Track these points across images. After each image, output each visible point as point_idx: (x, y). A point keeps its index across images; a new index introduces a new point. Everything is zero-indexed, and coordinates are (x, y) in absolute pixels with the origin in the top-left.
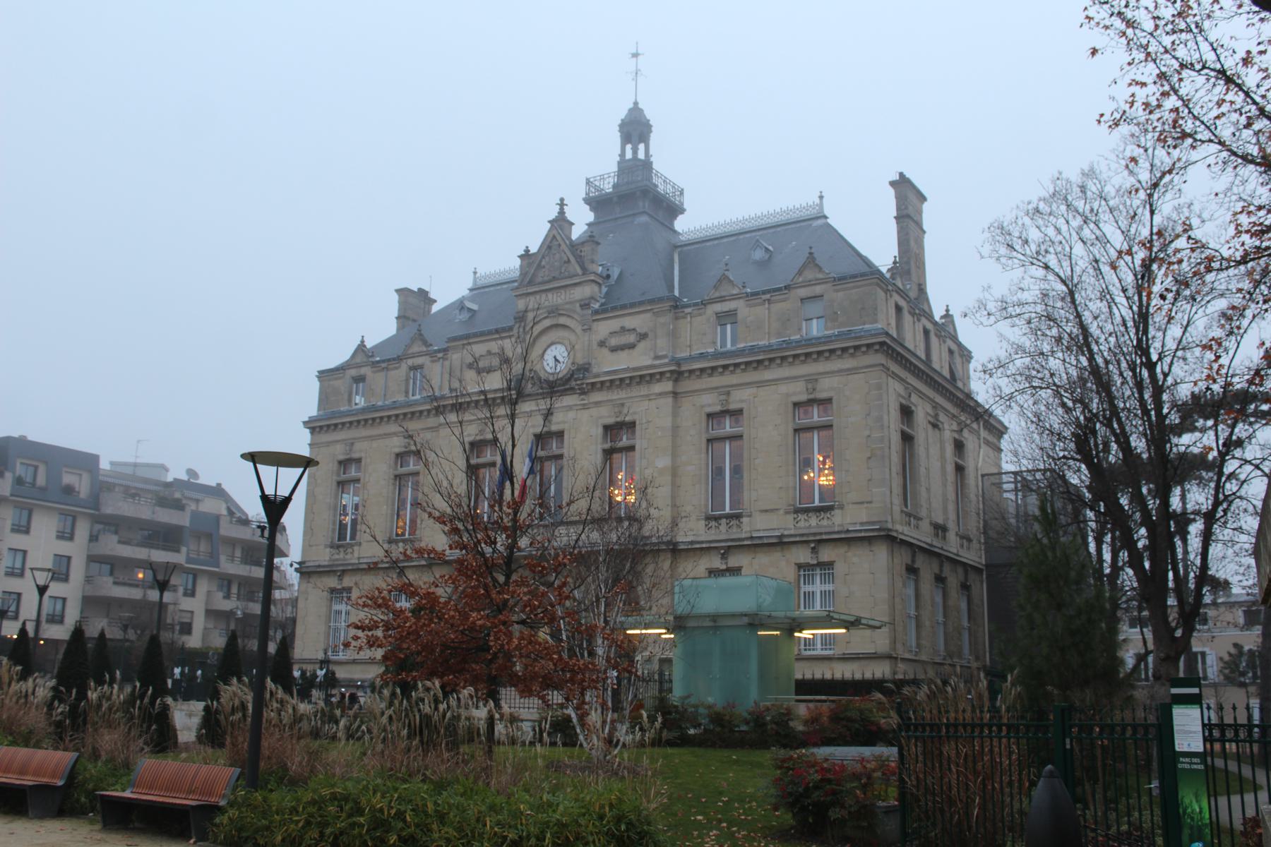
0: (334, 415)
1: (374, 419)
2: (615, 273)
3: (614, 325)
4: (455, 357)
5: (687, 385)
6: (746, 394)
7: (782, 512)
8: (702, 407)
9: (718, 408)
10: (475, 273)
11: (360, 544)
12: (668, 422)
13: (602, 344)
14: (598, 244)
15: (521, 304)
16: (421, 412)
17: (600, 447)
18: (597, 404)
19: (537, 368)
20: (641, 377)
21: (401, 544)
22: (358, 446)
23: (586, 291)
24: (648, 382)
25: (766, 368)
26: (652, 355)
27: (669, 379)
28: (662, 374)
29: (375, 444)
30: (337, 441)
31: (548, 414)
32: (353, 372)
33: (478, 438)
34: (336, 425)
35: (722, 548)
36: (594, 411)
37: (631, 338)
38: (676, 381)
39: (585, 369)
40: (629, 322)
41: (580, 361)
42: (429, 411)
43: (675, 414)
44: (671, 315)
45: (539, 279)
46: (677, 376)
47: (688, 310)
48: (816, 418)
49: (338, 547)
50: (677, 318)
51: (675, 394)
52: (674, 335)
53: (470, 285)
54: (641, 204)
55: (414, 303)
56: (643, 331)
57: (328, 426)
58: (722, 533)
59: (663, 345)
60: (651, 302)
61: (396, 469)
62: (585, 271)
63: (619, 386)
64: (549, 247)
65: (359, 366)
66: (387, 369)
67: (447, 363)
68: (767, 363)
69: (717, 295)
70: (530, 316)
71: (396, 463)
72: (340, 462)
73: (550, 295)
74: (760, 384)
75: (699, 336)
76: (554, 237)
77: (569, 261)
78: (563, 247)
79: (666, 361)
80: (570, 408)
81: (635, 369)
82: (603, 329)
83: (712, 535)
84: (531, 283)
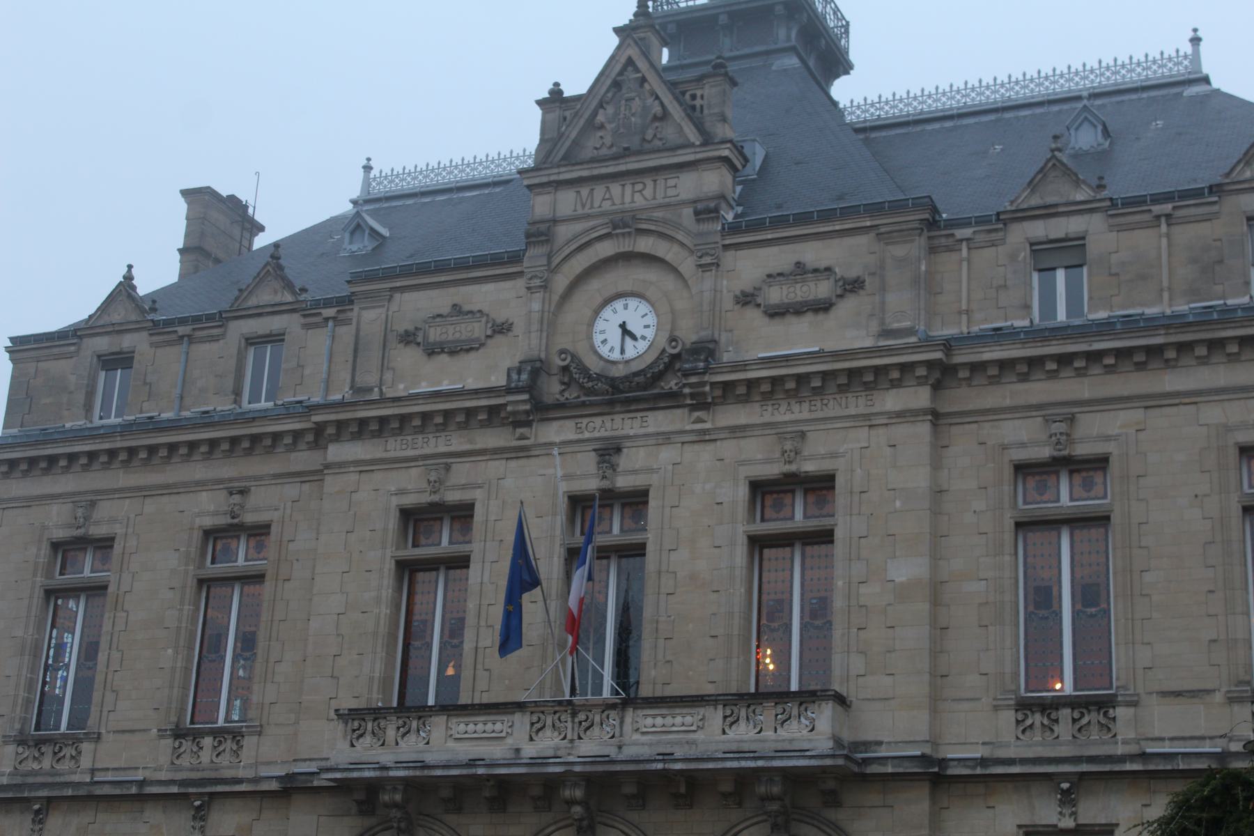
0: (46, 438)
1: (152, 450)
2: (757, 155)
3: (779, 258)
4: (370, 318)
5: (964, 397)
6: (1118, 422)
7: (1218, 697)
8: (1004, 447)
9: (1045, 453)
10: (367, 168)
11: (98, 738)
12: (920, 479)
13: (746, 299)
14: (734, 83)
15: (542, 205)
16: (276, 437)
17: (741, 530)
18: (737, 431)
19: (582, 350)
20: (851, 373)
21: (208, 741)
22: (105, 509)
23: (713, 181)
24: (868, 387)
25: (1168, 364)
26: (874, 327)
27: (921, 381)
28: (905, 368)
29: (150, 506)
30: (59, 496)
31: (609, 452)
32: (102, 344)
33: (426, 498)
34: (52, 460)
35: (1065, 776)
36: (728, 449)
37: (822, 289)
38: (937, 387)
39: (705, 350)
40: (812, 254)
41: (689, 334)
42: (297, 435)
43: (936, 464)
44: (922, 241)
45: (588, 153)
46: (942, 374)
47: (961, 233)
49: (39, 743)
50: (933, 250)
51: (936, 417)
52: (928, 286)
53: (356, 192)
54: (782, 33)
55: (217, 221)
56: (852, 274)
57: (32, 461)
58: (1062, 741)
59: (901, 306)
60: (875, 209)
61: (201, 565)
62: (708, 140)
63: (794, 395)
64: (617, 85)
65: (118, 330)
66: (191, 339)
67: (346, 333)
68: (1171, 354)
69: (1035, 201)
70: (564, 232)
71: (203, 554)
72: (56, 546)
73: (616, 189)
74: (1152, 401)
75: (987, 293)
76: (630, 62)
77: (664, 116)
78: (654, 82)
79: (913, 339)
80: (665, 438)
81: (837, 355)
82: (749, 266)
83: (1036, 746)
84: (569, 159)
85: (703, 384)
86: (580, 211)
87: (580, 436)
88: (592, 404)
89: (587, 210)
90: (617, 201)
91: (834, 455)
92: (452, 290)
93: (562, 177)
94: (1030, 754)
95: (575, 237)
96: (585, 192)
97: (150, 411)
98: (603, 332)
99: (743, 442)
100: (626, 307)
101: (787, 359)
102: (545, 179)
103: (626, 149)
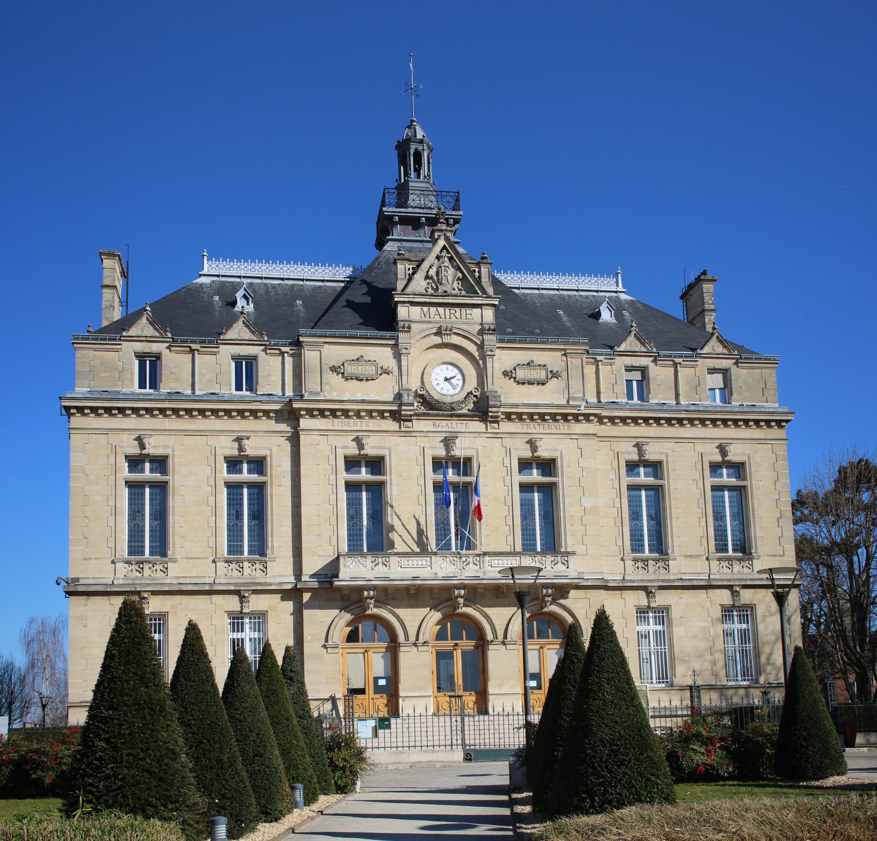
29: (188, 441)
34: (122, 410)
36: (508, 442)
40: (539, 357)
48: (725, 478)
73: (441, 310)
85: (497, 412)
86: (423, 318)
87: (435, 430)
88: (442, 415)
89: (427, 319)
90: (443, 316)
91: (555, 450)
92: (357, 347)
93: (415, 300)
94: (639, 578)
95: (423, 330)
96: (425, 309)
97: (174, 387)
98: (436, 379)
99: (514, 440)
100: (447, 369)
101: (536, 405)
102: (406, 300)
103: (445, 292)
